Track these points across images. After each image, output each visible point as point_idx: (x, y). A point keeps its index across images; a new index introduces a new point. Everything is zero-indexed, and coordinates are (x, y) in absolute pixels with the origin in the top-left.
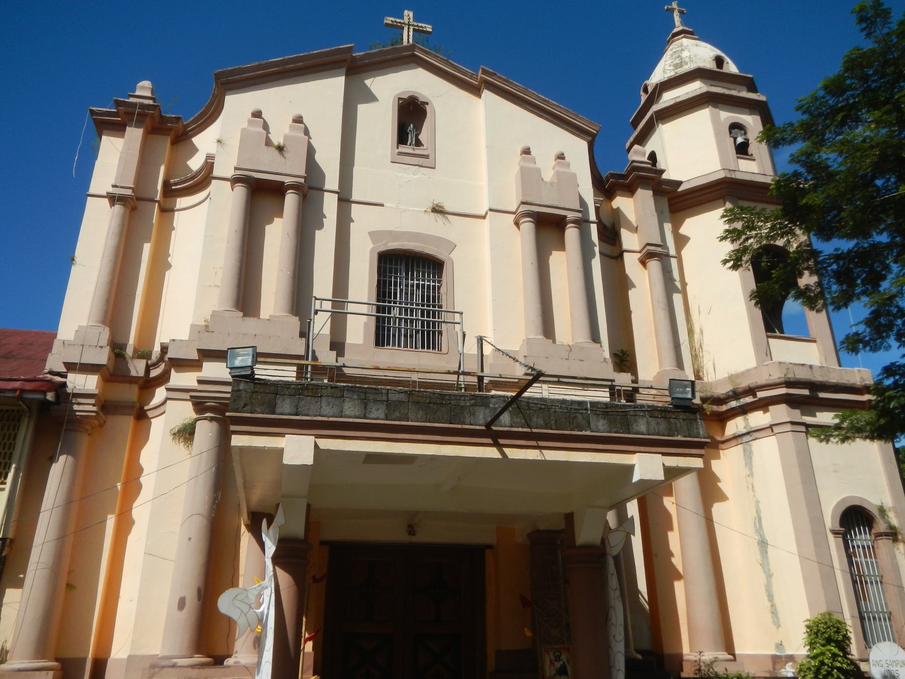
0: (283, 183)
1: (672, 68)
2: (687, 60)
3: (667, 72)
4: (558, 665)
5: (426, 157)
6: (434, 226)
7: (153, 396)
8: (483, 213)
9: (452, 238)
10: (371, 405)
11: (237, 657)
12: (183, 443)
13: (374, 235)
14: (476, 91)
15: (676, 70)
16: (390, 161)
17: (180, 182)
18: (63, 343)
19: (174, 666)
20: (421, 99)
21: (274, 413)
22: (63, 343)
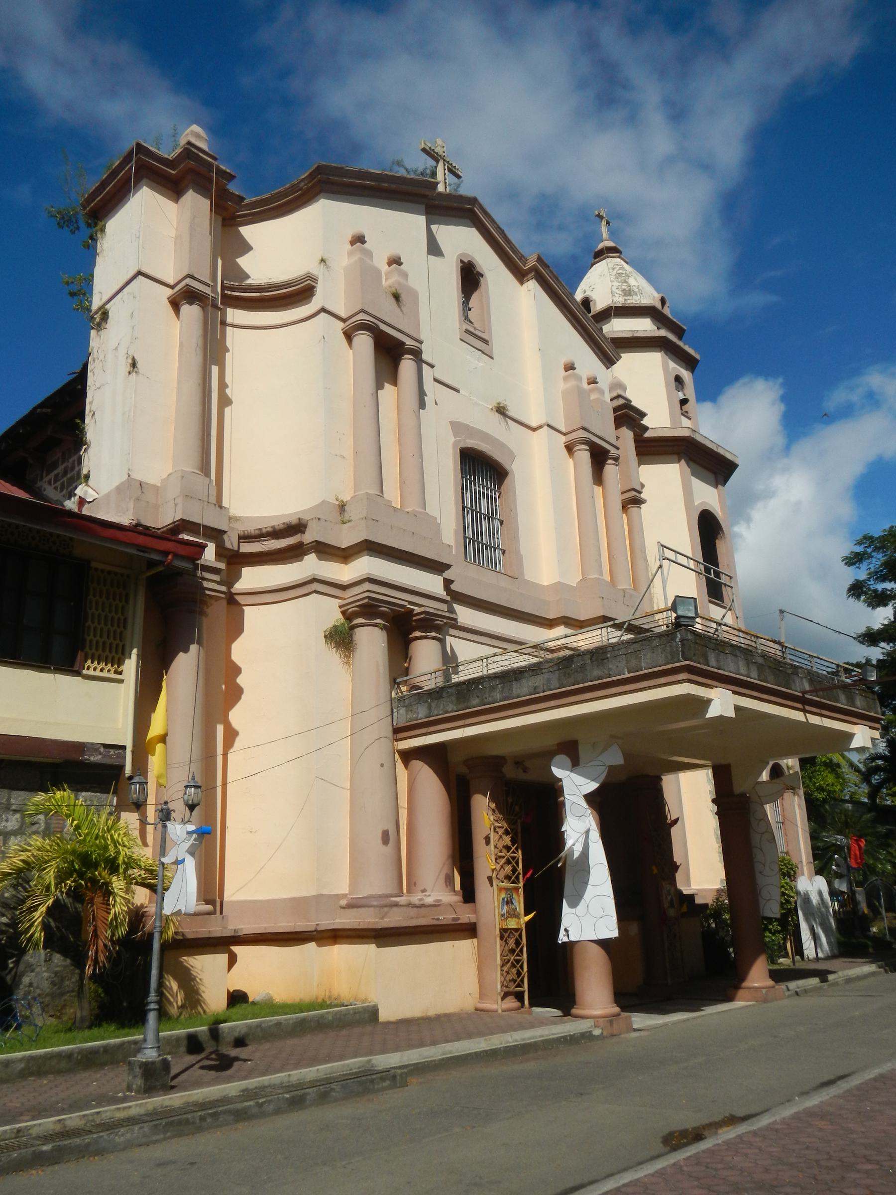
0: (403, 344)
1: (621, 293)
2: (636, 290)
3: (616, 295)
4: (669, 898)
5: (486, 342)
6: (494, 426)
7: (238, 576)
8: (534, 425)
9: (512, 446)
10: (750, 665)
11: (430, 896)
12: (335, 649)
13: (457, 427)
14: (521, 275)
15: (626, 298)
16: (458, 337)
17: (237, 288)
18: (140, 484)
19: (396, 905)
20: (478, 269)
21: (708, 666)
22: (140, 484)
